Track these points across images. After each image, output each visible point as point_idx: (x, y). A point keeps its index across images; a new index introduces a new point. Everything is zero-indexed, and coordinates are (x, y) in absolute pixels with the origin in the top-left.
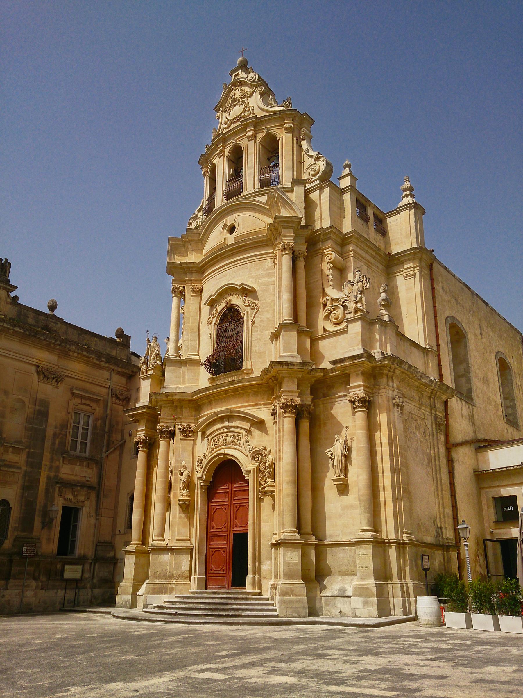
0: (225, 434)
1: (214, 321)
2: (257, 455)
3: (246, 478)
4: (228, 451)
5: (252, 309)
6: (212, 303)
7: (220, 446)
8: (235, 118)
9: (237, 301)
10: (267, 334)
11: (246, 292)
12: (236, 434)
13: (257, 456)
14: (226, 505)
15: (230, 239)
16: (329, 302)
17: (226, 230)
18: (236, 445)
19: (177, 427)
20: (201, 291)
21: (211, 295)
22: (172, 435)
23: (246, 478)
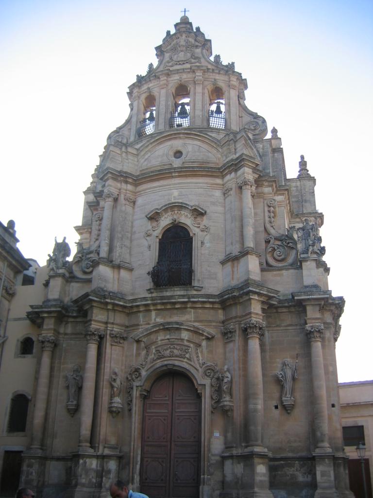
0: (172, 347)
1: (156, 233)
2: (210, 371)
3: (199, 392)
4: (177, 363)
5: (202, 231)
6: (154, 217)
7: (165, 357)
8: (182, 61)
9: (186, 219)
10: (222, 257)
11: (199, 213)
12: (186, 348)
13: (209, 371)
14: (167, 416)
15: (177, 163)
16: (272, 241)
17: (172, 153)
18: (184, 358)
19: (108, 332)
20: (134, 203)
21: (157, 209)
22: (101, 338)
23: (199, 392)
